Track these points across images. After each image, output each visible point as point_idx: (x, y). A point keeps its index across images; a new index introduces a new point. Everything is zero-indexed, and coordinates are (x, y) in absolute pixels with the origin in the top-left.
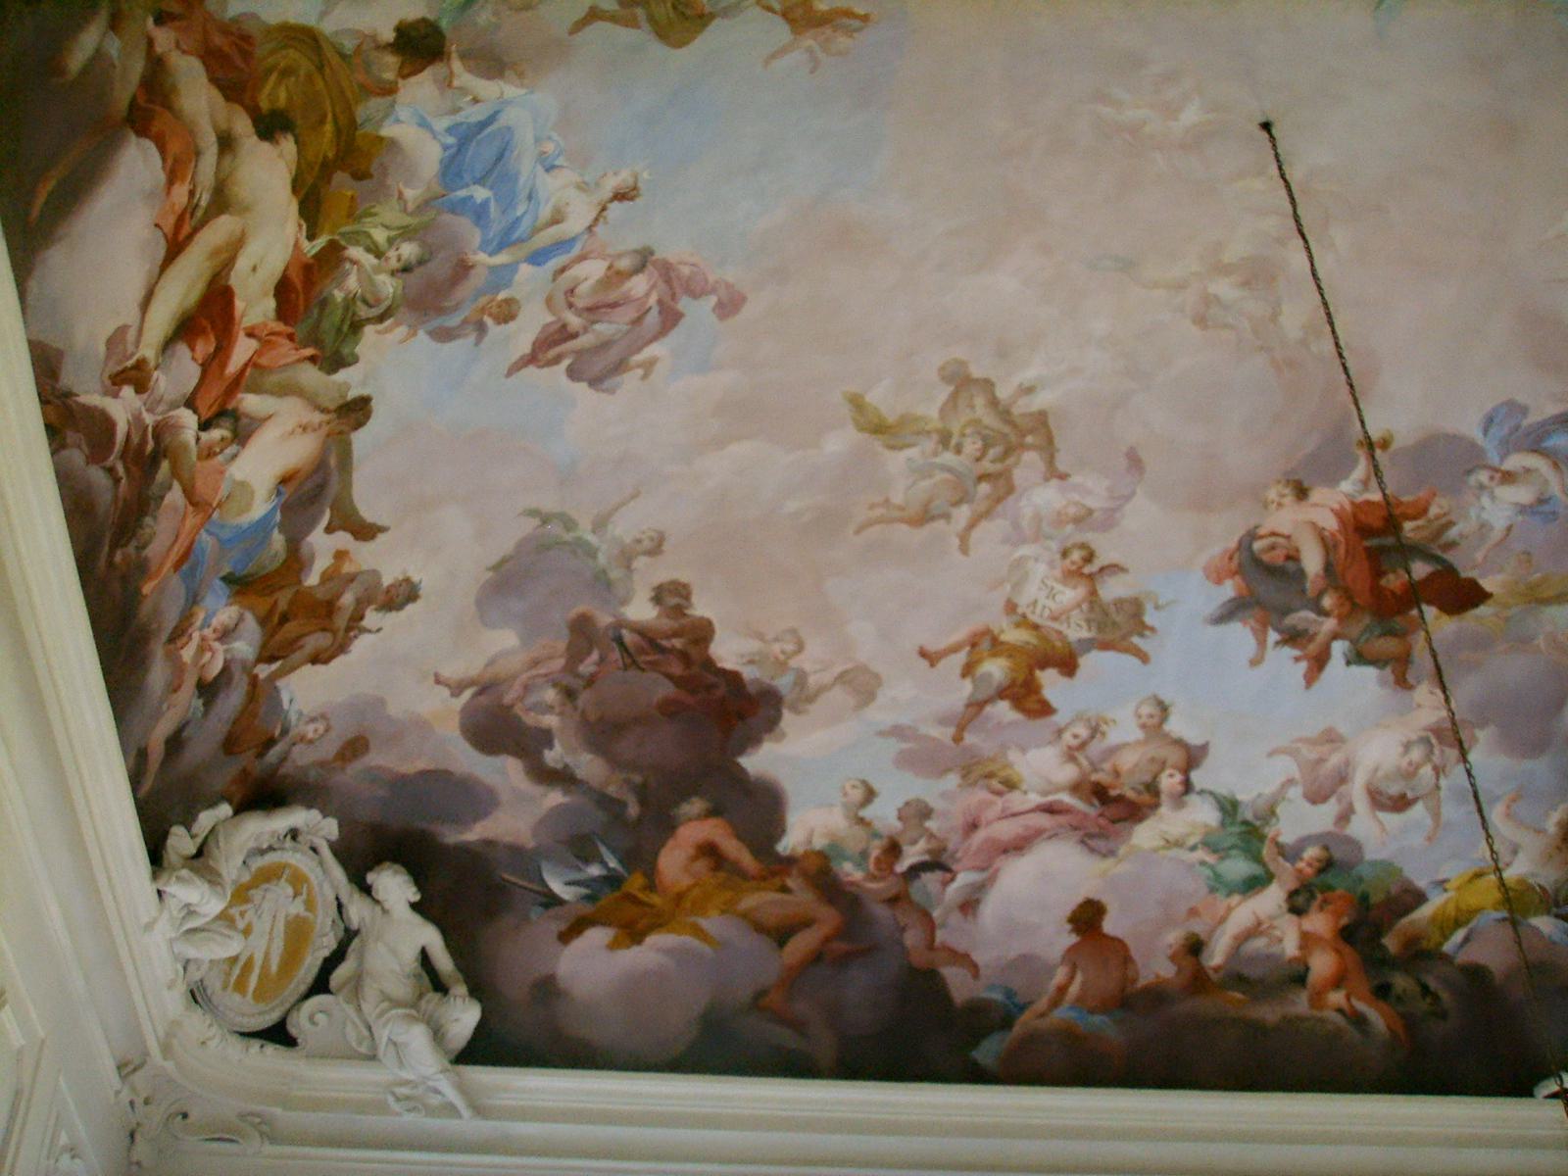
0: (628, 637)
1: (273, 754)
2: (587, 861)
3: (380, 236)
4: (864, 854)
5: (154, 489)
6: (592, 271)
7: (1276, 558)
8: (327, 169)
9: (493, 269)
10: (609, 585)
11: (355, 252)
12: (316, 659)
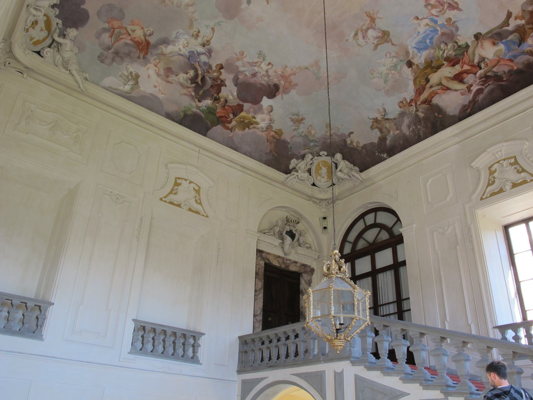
3: (441, 52)
5: (493, 75)
6: (434, 12)
8: (433, 68)
9: (441, 29)
11: (445, 55)
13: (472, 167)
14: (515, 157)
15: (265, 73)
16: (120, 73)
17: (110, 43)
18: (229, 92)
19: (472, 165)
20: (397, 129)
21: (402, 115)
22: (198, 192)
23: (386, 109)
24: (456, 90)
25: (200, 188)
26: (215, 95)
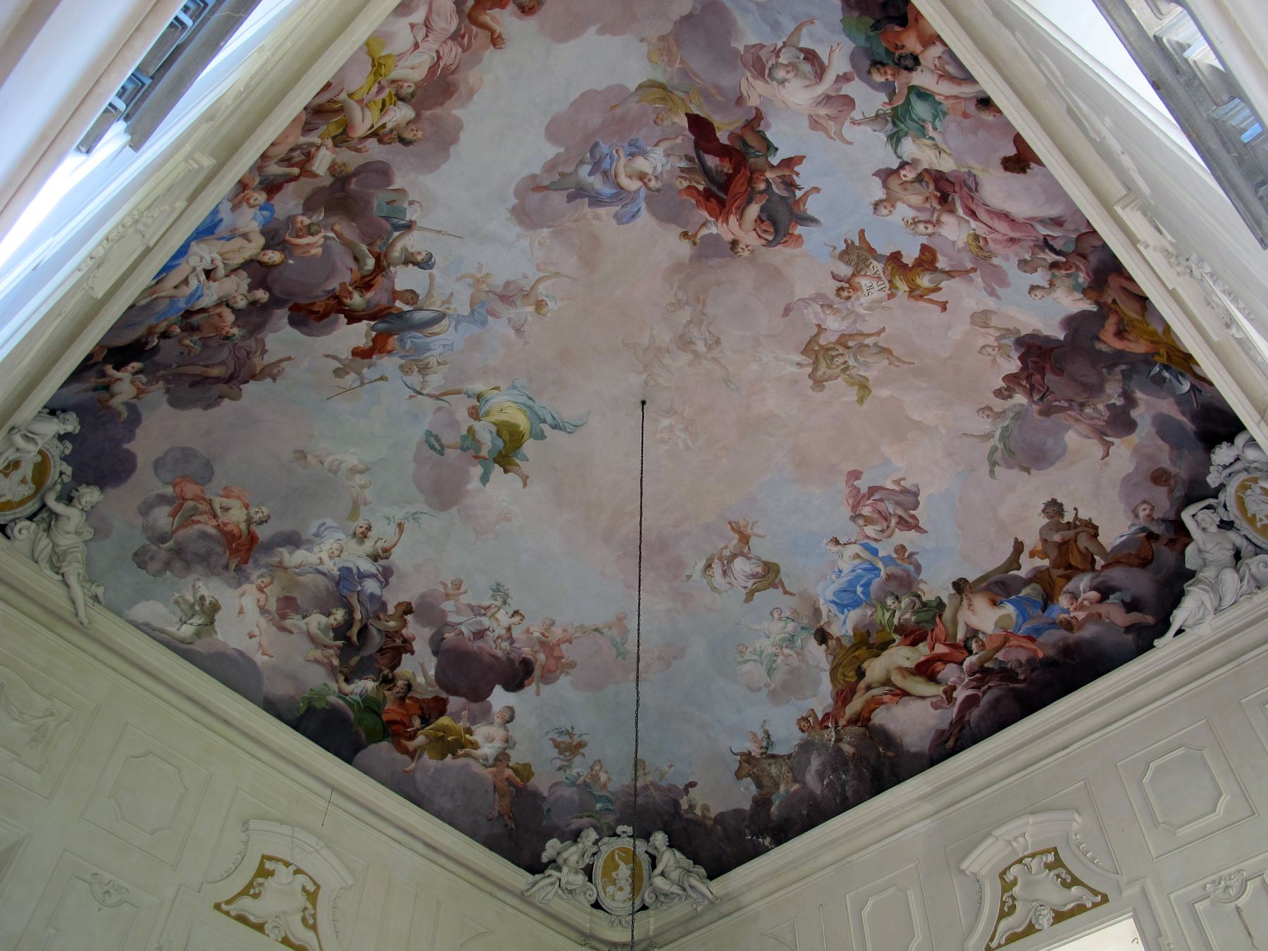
0: (1036, 398)
1: (1156, 529)
2: (1164, 379)
3: (887, 615)
4: (1068, 276)
5: (996, 668)
6: (870, 530)
7: (767, 226)
8: (870, 647)
9: (886, 566)
10: (1018, 413)
11: (896, 621)
12: (1096, 535)
13: (963, 872)
14: (1055, 850)
15: (503, 632)
16: (177, 595)
17: (168, 529)
18: (419, 667)
19: (963, 866)
20: (795, 781)
21: (806, 747)
22: (312, 897)
23: (771, 732)
24: (923, 698)
25: (318, 887)
26: (386, 672)
